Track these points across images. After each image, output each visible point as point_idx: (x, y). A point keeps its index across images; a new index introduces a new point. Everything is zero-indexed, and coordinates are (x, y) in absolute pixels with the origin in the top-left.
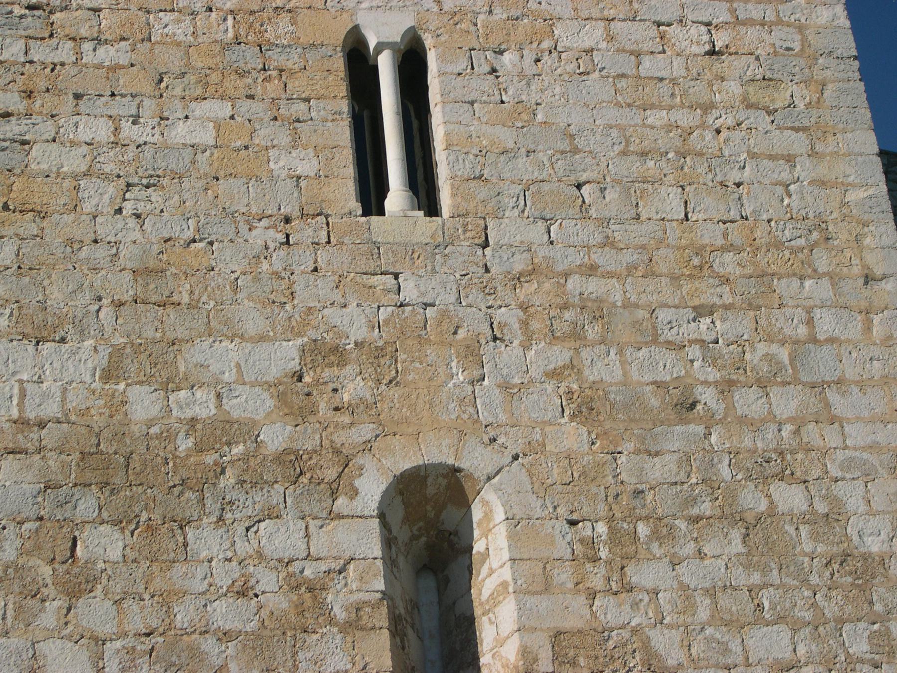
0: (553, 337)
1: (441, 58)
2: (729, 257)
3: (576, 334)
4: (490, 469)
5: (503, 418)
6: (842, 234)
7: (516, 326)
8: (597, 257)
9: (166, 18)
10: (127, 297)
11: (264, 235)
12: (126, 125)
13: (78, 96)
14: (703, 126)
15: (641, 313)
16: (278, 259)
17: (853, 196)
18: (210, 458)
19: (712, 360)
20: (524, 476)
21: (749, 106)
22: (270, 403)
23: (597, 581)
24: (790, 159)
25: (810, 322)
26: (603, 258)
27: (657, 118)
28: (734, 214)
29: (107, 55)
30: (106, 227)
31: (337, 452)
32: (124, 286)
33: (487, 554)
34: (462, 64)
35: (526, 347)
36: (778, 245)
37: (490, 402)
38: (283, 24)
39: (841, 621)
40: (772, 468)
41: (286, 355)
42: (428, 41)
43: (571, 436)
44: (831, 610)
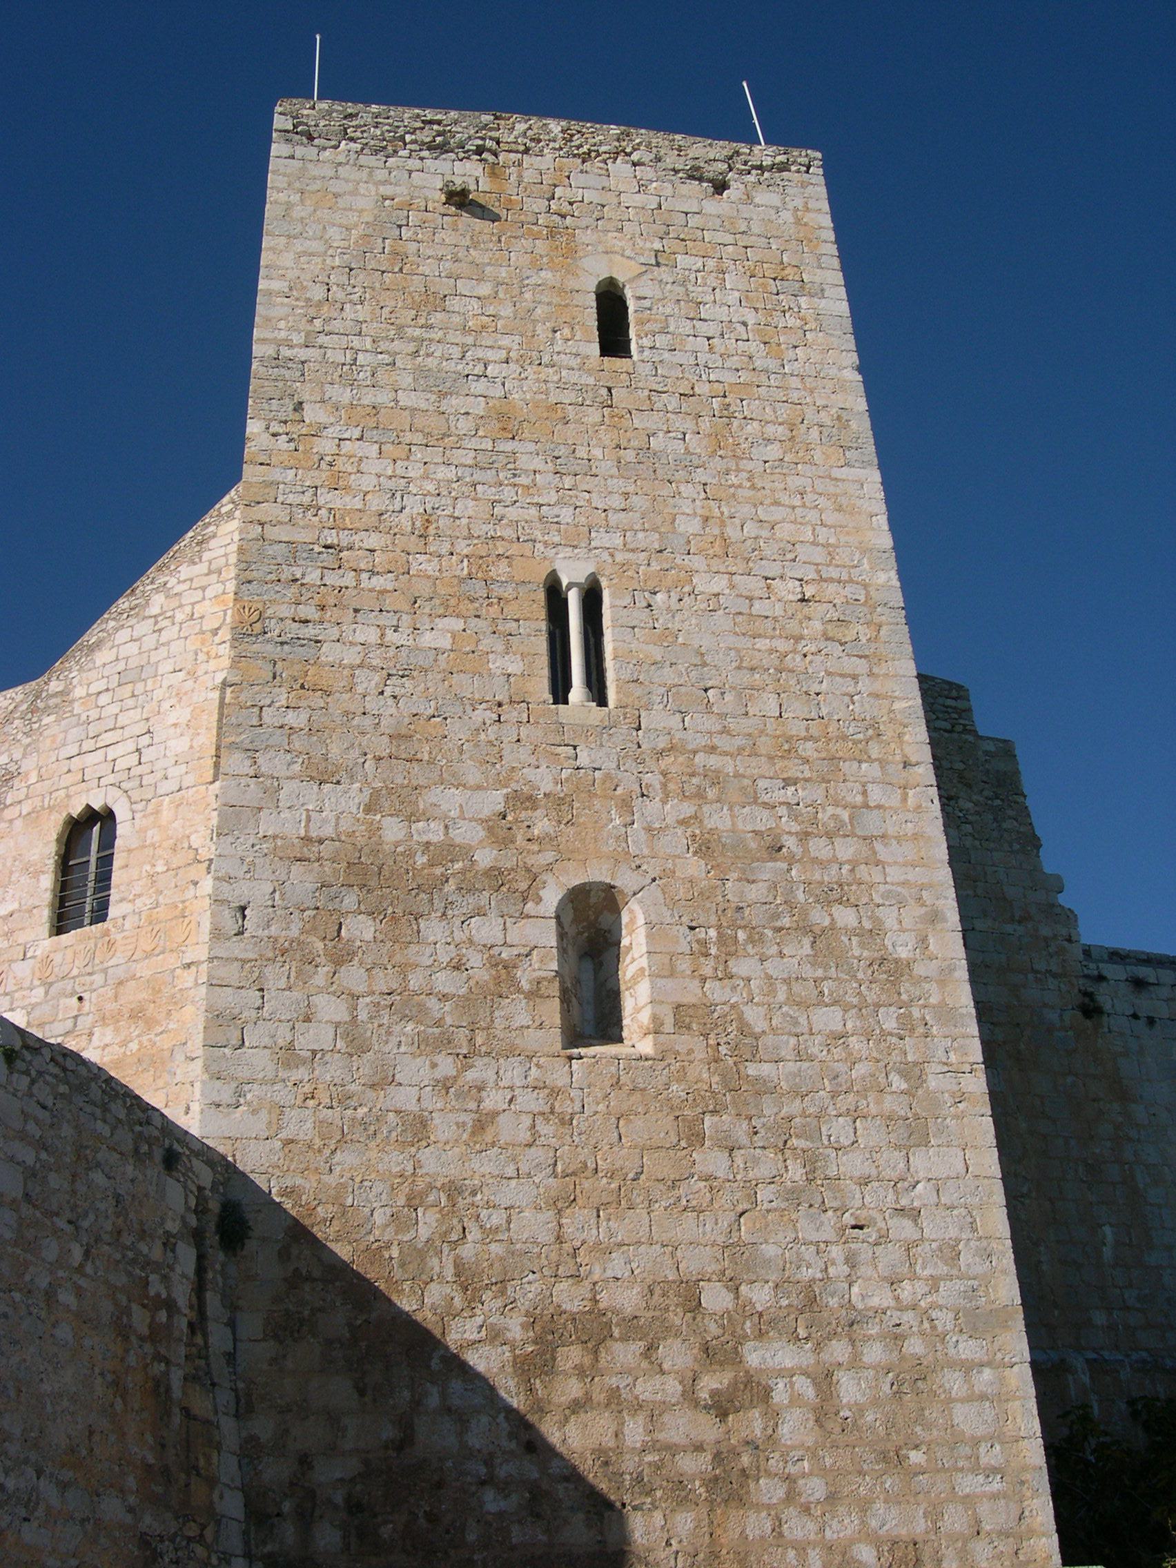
1: (613, 595)
3: (700, 795)
4: (636, 888)
5: (646, 852)
6: (889, 732)
7: (658, 786)
8: (716, 741)
9: (421, 558)
11: (483, 714)
12: (389, 632)
13: (356, 611)
14: (794, 651)
15: (746, 782)
16: (492, 732)
17: (898, 706)
18: (438, 871)
19: (795, 817)
20: (659, 894)
21: (827, 639)
22: (482, 834)
23: (707, 968)
24: (855, 677)
25: (864, 793)
27: (763, 644)
28: (814, 715)
29: (378, 582)
30: (372, 704)
31: (528, 870)
32: (383, 746)
33: (630, 948)
34: (627, 600)
35: (664, 802)
36: (844, 738)
37: (637, 839)
38: (503, 567)
39: (877, 1006)
40: (834, 895)
41: (494, 800)
42: (604, 583)
43: (694, 867)
44: (871, 997)
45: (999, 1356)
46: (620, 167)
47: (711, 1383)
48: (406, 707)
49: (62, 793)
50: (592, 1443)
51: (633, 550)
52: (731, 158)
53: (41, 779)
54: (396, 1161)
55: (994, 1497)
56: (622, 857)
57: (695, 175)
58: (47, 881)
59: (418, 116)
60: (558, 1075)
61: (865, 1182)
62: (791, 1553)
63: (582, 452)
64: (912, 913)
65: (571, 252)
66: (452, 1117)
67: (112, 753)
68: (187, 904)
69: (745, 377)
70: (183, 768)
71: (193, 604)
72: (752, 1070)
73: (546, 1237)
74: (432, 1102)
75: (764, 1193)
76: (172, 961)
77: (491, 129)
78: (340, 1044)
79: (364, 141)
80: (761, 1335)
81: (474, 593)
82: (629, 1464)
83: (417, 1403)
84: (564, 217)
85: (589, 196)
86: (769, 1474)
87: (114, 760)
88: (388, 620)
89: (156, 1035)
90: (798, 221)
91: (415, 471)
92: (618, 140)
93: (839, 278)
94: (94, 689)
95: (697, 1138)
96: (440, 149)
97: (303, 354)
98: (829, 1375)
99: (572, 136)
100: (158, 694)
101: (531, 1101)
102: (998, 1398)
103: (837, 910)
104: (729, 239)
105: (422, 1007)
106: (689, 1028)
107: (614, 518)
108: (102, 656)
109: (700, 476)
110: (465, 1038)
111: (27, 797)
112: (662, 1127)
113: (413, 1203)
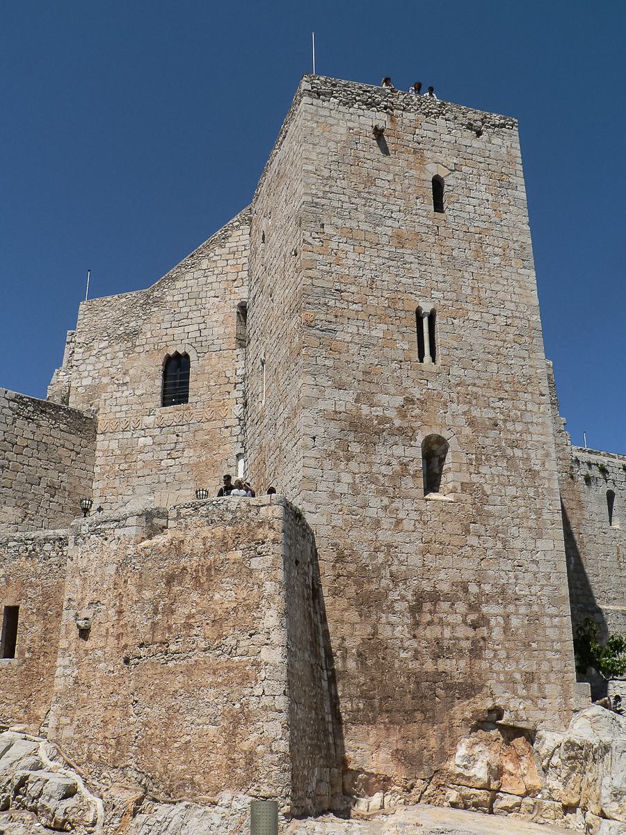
0: (465, 403)
6: (535, 381)
11: (394, 365)
13: (349, 319)
14: (503, 346)
18: (381, 427)
24: (524, 358)
26: (477, 381)
27: (492, 343)
30: (356, 358)
36: (520, 382)
37: (449, 421)
40: (514, 445)
41: (399, 400)
43: (467, 430)
45: (561, 613)
46: (440, 121)
47: (472, 617)
48: (368, 361)
49: (164, 344)
50: (434, 636)
52: (482, 119)
53: (153, 336)
54: (370, 535)
55: (558, 659)
56: (443, 425)
57: (470, 126)
58: (159, 382)
59: (361, 87)
62: (495, 675)
64: (541, 452)
65: (422, 160)
66: (387, 520)
67: (187, 329)
68: (226, 400)
69: (487, 225)
70: (221, 341)
71: (222, 267)
72: (486, 508)
73: (419, 564)
74: (381, 514)
76: (220, 424)
77: (390, 97)
78: (350, 492)
79: (340, 99)
80: (487, 602)
81: (390, 313)
82: (445, 643)
84: (419, 144)
85: (430, 134)
86: (489, 649)
89: (214, 455)
90: (508, 153)
91: (368, 260)
92: (440, 107)
93: (522, 181)
94: (176, 298)
95: (467, 531)
96: (370, 105)
97: (323, 201)
98: (508, 616)
99: (422, 103)
103: (516, 450)
104: (482, 160)
105: (377, 478)
107: (440, 285)
108: (179, 284)
109: (471, 269)
110: (391, 491)
111: (146, 343)
112: (454, 527)
113: (377, 550)
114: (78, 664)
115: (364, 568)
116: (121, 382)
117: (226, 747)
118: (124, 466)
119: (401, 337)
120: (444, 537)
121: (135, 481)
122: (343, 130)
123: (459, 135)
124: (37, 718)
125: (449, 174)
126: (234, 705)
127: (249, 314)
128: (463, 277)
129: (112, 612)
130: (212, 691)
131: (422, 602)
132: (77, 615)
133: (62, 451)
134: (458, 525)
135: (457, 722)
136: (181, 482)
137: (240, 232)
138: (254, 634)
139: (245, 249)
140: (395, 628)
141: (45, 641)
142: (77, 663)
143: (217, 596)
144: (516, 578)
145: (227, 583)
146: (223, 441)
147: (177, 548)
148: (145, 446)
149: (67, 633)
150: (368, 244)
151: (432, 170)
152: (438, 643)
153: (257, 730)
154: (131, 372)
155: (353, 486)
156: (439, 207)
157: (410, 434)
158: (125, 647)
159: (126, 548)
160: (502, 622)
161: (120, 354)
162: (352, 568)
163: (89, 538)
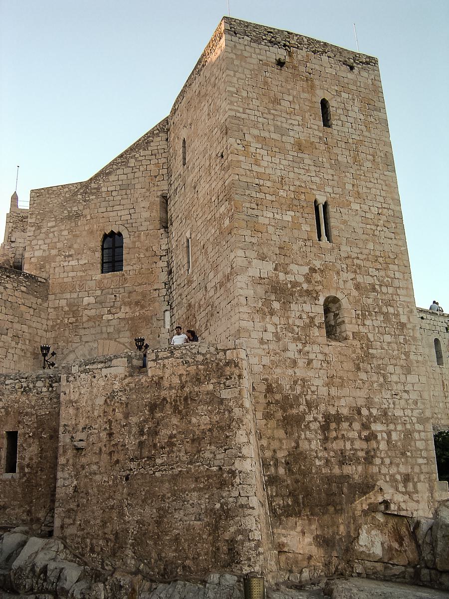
2: (381, 258)
3: (355, 272)
7: (345, 268)
10: (278, 253)
11: (301, 243)
13: (267, 207)
18: (294, 290)
23: (359, 323)
24: (391, 239)
25: (394, 274)
26: (360, 256)
27: (368, 226)
30: (274, 238)
35: (347, 273)
39: (399, 335)
40: (388, 304)
41: (305, 270)
43: (355, 293)
47: (365, 433)
50: (339, 448)
51: (336, 194)
55: (425, 464)
56: (338, 289)
57: (345, 63)
58: (98, 255)
60: (326, 350)
61: (396, 383)
63: (320, 160)
65: (312, 87)
72: (371, 351)
74: (297, 356)
75: (375, 385)
76: (149, 288)
80: (375, 422)
83: (299, 437)
84: (310, 74)
85: (317, 67)
86: (378, 457)
87: (121, 216)
88: (275, 210)
90: (373, 84)
95: (359, 369)
97: (243, 116)
98: (390, 432)
100: (136, 195)
101: (321, 357)
102: (426, 440)
105: (293, 330)
106: (356, 339)
107: (331, 183)
108: (112, 178)
113: (295, 382)
114: (77, 476)
115: (286, 398)
116: (67, 254)
117: (211, 538)
118: (72, 320)
119: (304, 222)
120: (341, 373)
121: (82, 332)
122: (255, 61)
123: (338, 69)
124: (38, 519)
125: (332, 98)
126: (215, 504)
127: (171, 203)
128: (346, 176)
129: (103, 435)
130: (195, 494)
131: (330, 422)
132: (72, 437)
133: (23, 308)
134: (351, 364)
135: (358, 513)
136: (119, 332)
137: (159, 139)
138: (228, 449)
139: (164, 152)
140: (311, 442)
141: (41, 459)
142: (75, 476)
143: (194, 420)
144: (394, 403)
145: (202, 409)
146: (153, 300)
147: (158, 383)
148: (89, 304)
149: (65, 452)
150: (277, 150)
151: (320, 95)
152: (342, 453)
153: (236, 523)
154: (75, 246)
155: (276, 334)
156: (327, 122)
157: (315, 295)
158: (117, 462)
159: (113, 384)
160: (386, 437)
161: (65, 233)
162: (278, 397)
163: (79, 376)
